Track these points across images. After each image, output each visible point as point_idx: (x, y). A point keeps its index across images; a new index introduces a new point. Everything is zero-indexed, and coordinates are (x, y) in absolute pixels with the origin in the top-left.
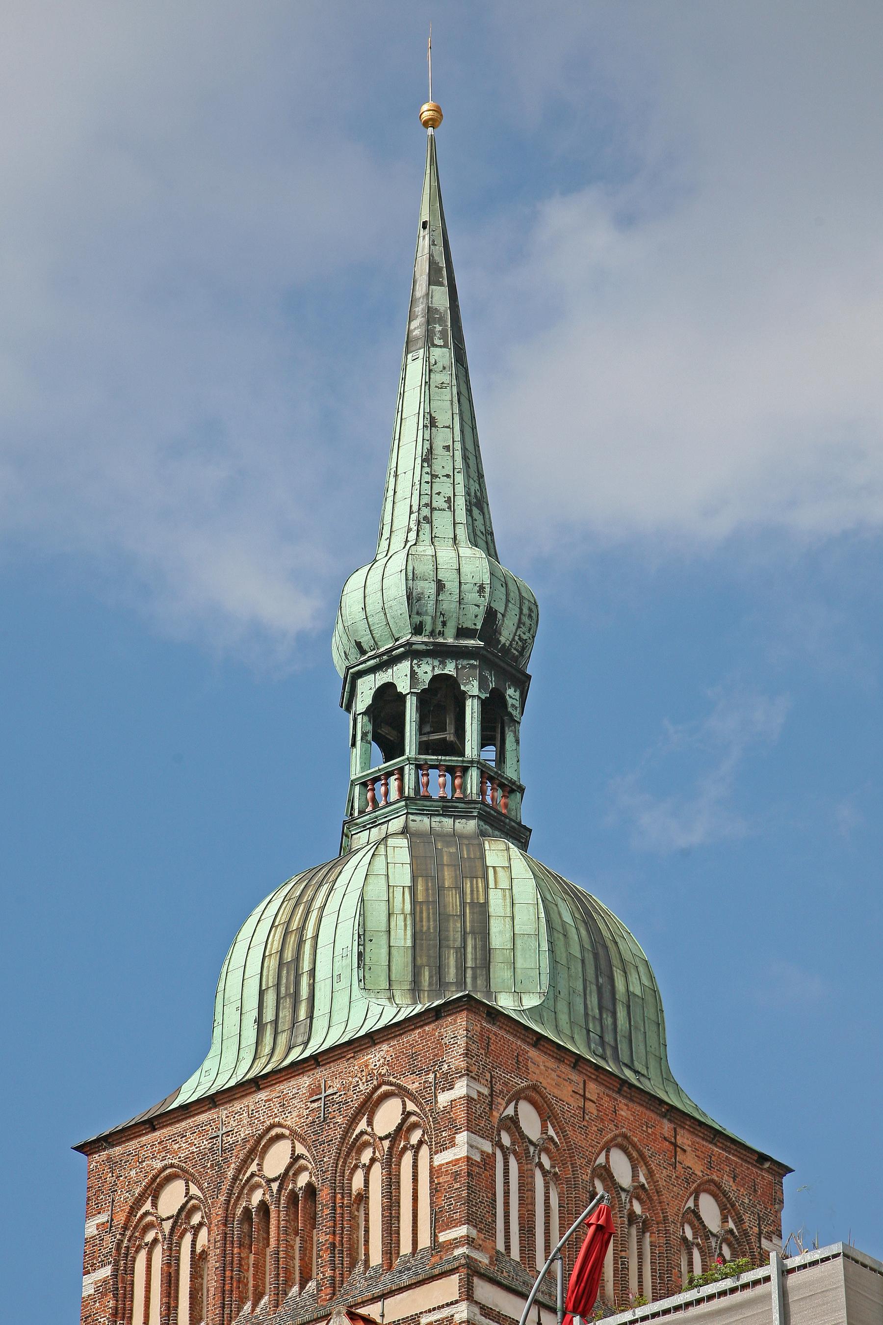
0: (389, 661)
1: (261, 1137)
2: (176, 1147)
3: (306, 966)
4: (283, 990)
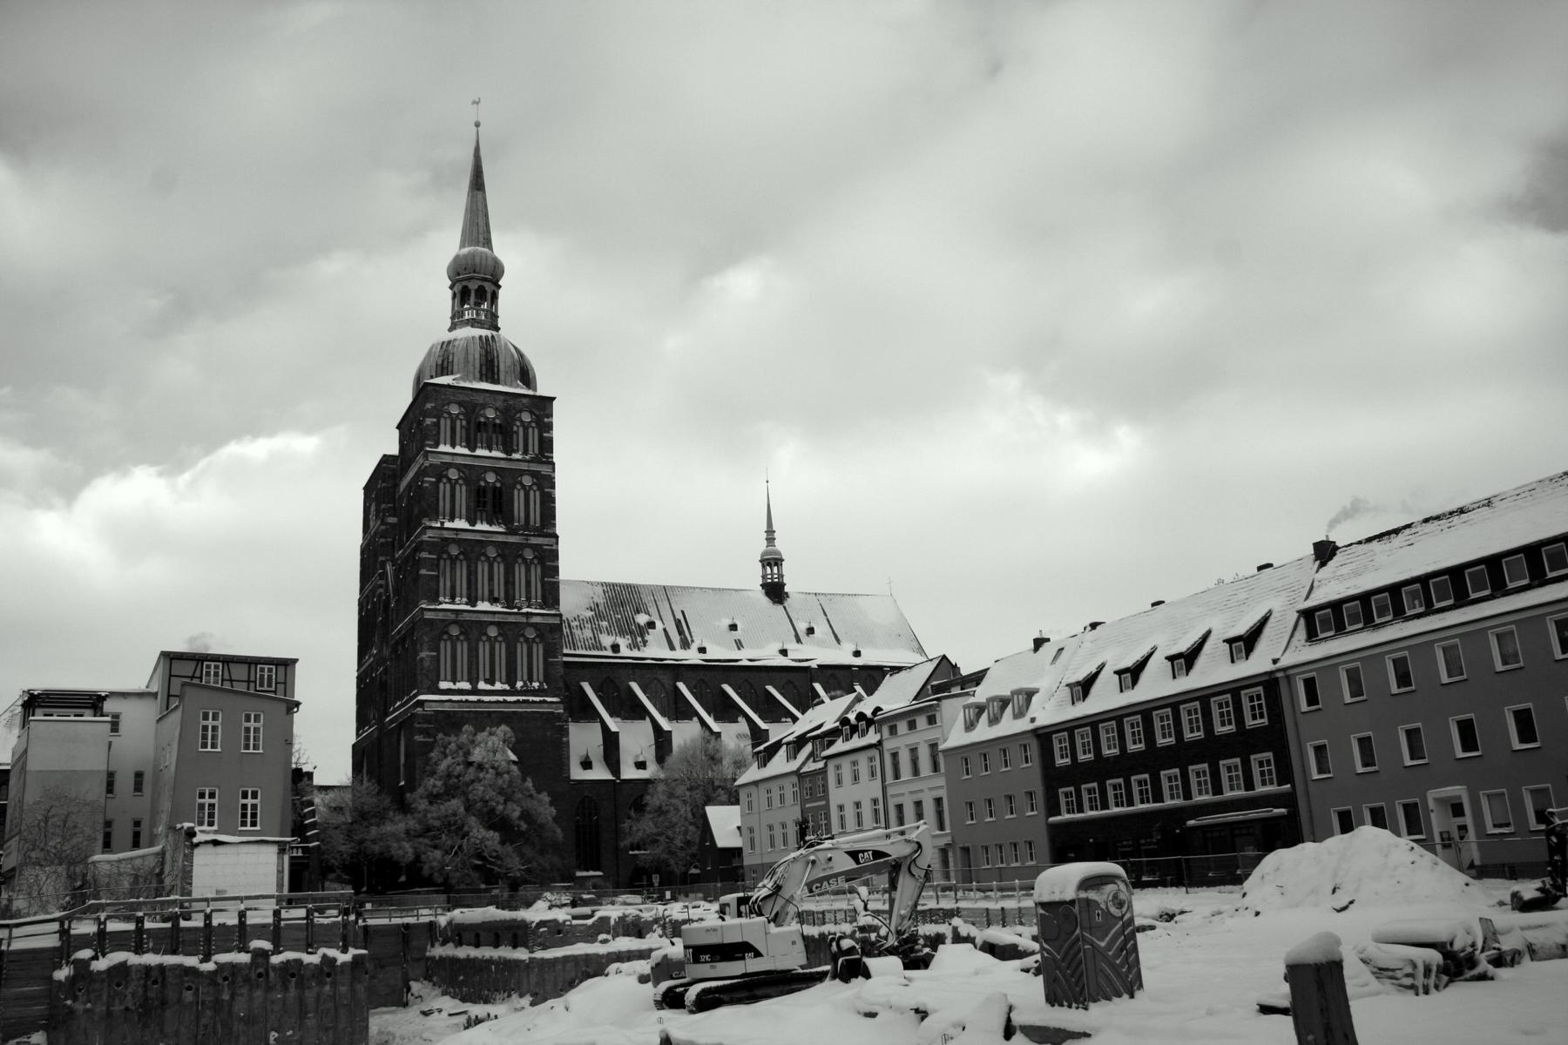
0: (485, 280)
3: (496, 364)
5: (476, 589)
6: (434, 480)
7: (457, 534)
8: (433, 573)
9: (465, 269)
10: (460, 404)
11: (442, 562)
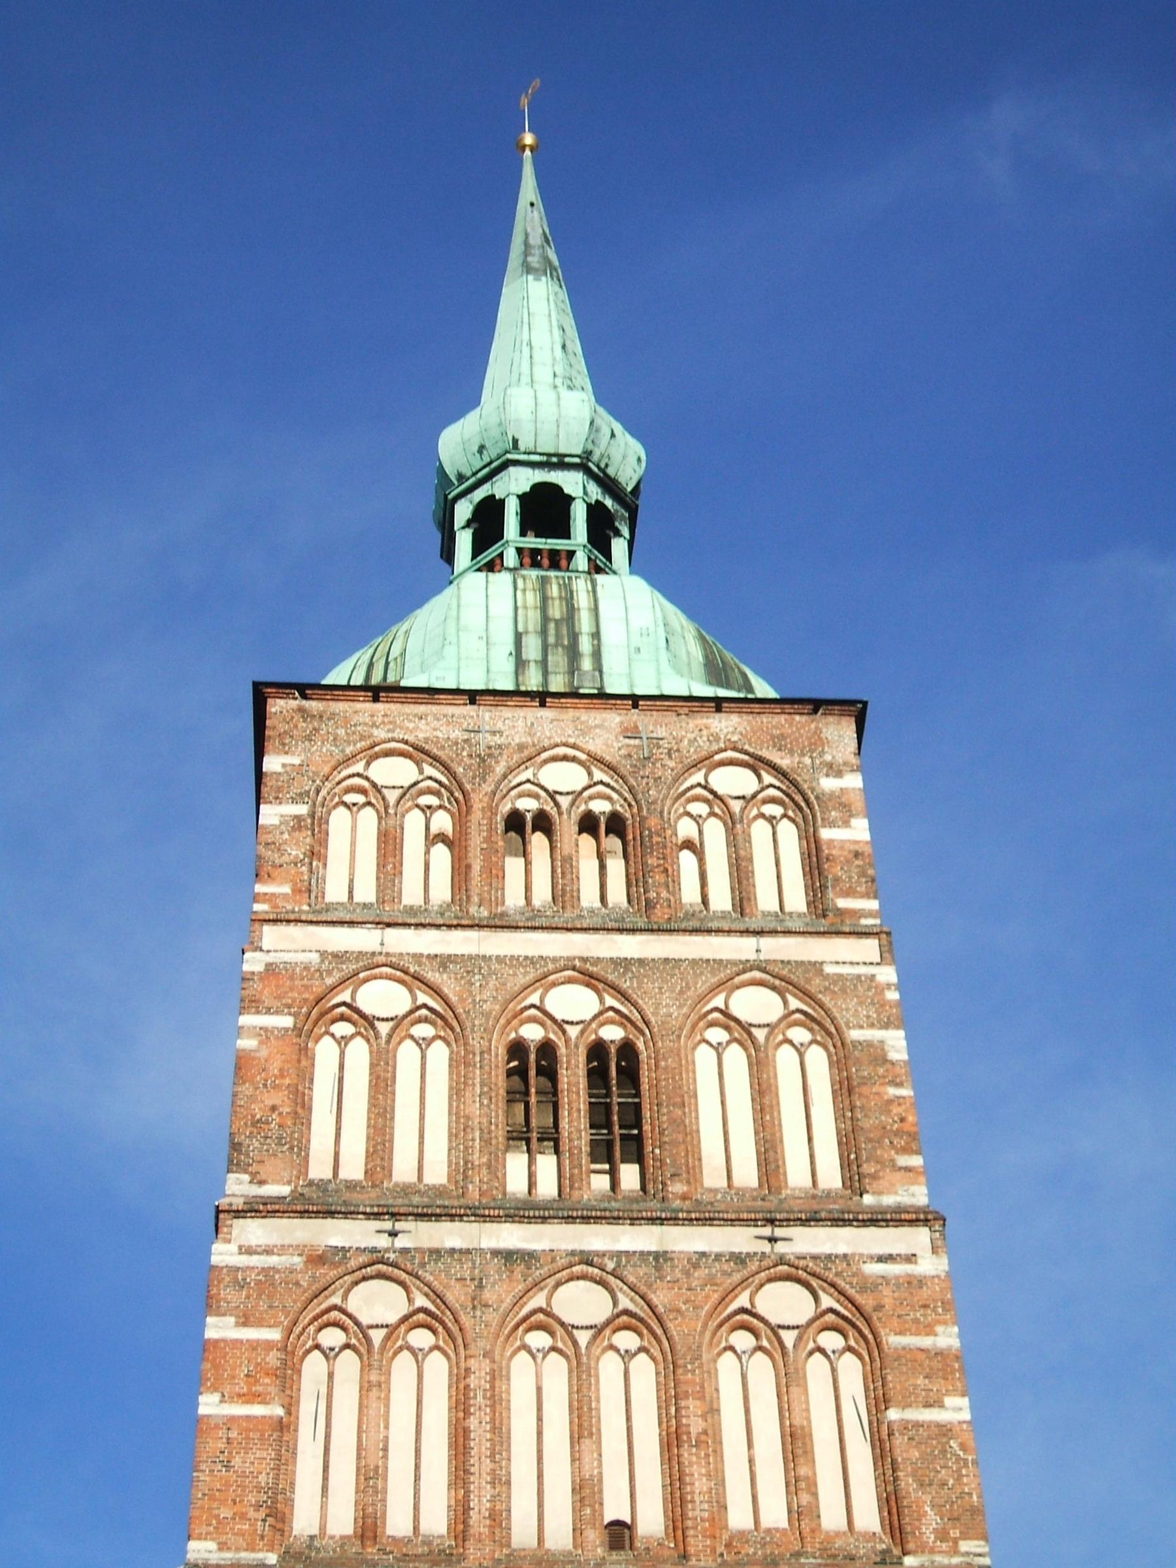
1: (545, 750)
2: (411, 726)
4: (551, 640)
5: (502, 1481)
6: (287, 1021)
7: (393, 1234)
8: (258, 1410)
9: (481, 449)
10: (419, 753)
11: (314, 1365)
